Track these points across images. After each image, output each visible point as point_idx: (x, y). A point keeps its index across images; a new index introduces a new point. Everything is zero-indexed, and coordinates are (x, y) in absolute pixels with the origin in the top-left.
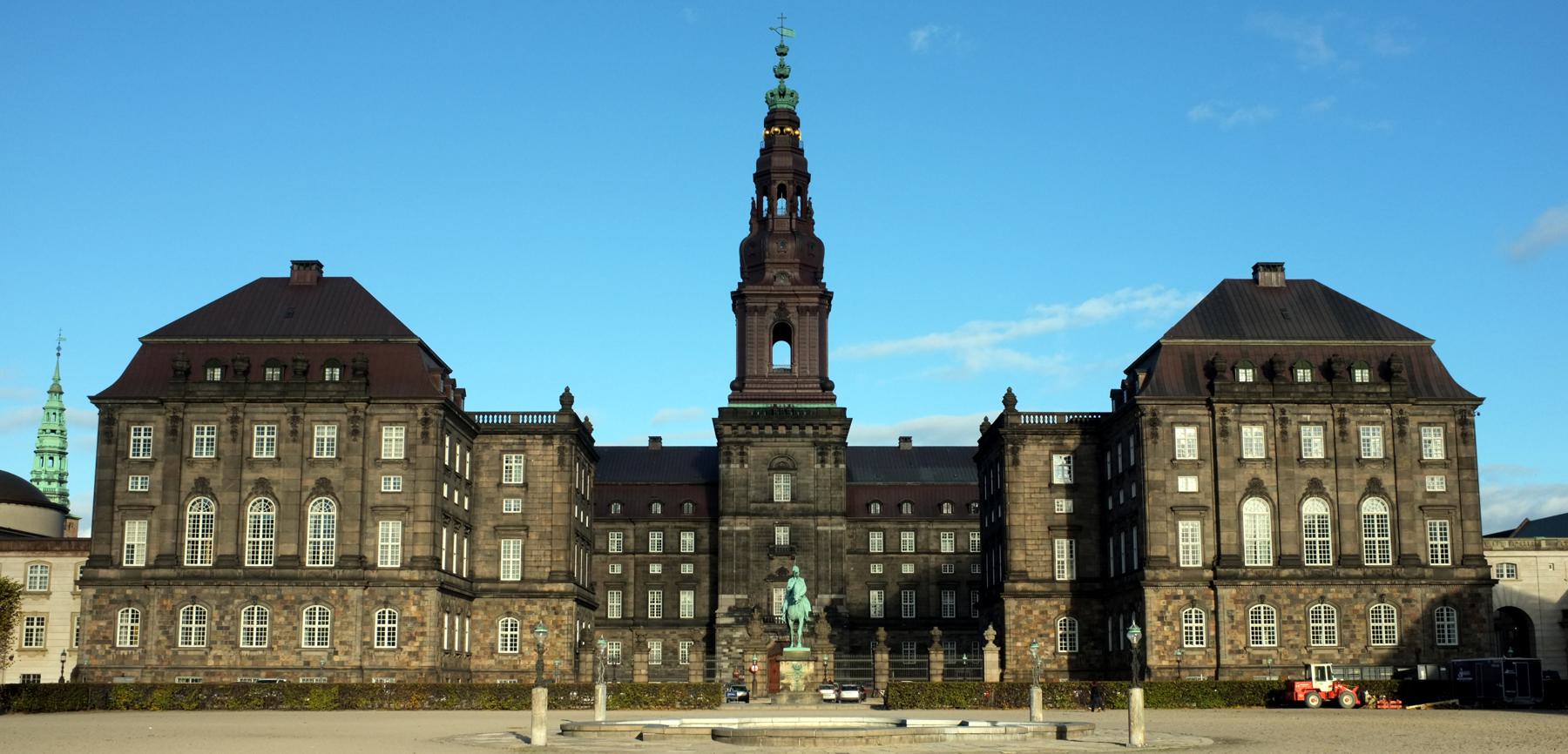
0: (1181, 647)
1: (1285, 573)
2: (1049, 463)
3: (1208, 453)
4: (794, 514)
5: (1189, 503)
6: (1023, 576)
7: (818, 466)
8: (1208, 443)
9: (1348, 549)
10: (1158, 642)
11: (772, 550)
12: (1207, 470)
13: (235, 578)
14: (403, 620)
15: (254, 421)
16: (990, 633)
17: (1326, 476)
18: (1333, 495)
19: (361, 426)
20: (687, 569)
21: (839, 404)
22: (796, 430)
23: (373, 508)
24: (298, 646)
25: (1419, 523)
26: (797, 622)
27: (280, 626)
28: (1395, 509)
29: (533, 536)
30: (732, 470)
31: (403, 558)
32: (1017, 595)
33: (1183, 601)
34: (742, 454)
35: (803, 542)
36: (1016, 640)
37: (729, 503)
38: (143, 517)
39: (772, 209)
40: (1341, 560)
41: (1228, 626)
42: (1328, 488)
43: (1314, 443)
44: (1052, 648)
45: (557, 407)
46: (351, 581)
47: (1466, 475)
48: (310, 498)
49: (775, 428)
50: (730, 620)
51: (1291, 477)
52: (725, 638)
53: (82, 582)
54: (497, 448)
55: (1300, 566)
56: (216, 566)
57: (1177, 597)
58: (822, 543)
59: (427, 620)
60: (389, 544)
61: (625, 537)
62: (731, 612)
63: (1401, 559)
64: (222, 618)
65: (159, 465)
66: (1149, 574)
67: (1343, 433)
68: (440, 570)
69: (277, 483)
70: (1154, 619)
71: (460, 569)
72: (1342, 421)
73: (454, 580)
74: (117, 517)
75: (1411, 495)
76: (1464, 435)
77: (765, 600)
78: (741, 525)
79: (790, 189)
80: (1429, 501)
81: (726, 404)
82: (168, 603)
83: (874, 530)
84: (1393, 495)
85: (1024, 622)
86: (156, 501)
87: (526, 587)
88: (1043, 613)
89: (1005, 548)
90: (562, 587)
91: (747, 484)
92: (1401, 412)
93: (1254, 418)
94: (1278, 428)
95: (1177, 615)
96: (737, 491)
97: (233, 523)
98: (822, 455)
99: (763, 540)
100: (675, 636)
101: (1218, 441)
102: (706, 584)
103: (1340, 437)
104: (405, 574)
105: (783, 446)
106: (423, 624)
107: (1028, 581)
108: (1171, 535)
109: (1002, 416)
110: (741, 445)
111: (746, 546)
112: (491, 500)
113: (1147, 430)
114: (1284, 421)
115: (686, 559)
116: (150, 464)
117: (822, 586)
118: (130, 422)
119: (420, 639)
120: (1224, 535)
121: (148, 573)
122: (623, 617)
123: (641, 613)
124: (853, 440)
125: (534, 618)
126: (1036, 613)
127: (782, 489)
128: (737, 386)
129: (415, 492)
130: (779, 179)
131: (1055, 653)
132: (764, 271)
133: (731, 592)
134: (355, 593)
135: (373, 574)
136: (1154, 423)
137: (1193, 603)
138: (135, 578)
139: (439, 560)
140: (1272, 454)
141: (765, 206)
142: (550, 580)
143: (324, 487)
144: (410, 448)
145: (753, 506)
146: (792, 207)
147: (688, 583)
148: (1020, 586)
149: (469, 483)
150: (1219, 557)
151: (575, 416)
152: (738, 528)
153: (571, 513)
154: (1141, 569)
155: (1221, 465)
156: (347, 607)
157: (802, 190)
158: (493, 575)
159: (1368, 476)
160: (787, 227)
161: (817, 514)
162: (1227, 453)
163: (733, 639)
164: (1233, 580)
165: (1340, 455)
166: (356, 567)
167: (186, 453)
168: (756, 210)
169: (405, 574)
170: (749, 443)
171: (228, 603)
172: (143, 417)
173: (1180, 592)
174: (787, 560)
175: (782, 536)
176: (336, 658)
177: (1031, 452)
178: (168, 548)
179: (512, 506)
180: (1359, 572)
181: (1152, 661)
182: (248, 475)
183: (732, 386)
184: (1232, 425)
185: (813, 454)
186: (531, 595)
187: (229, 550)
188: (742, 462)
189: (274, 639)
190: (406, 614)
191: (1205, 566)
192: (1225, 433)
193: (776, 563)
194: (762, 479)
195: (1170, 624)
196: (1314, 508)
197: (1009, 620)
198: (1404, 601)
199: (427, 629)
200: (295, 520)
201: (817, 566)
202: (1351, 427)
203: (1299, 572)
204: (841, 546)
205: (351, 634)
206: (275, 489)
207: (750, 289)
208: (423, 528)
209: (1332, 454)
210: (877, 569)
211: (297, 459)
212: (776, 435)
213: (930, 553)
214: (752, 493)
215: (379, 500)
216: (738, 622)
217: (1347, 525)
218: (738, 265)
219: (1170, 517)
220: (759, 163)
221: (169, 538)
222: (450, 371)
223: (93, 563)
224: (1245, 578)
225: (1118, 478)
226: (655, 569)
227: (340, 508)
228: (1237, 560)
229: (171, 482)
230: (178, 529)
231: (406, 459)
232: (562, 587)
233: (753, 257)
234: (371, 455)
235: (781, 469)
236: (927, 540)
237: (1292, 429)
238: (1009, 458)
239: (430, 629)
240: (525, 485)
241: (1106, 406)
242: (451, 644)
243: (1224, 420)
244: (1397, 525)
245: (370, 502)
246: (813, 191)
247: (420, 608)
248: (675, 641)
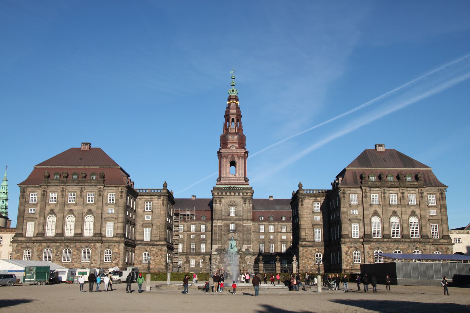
0: (353, 263)
1: (385, 240)
2: (312, 205)
3: (361, 203)
4: (236, 220)
5: (355, 218)
6: (305, 240)
7: (244, 205)
8: (361, 199)
9: (405, 233)
10: (346, 261)
11: (229, 231)
12: (361, 208)
13: (61, 240)
14: (113, 253)
15: (69, 192)
16: (295, 258)
17: (398, 210)
18: (400, 216)
19: (102, 193)
20: (203, 237)
22: (237, 194)
23: (105, 218)
24: (80, 261)
25: (428, 225)
26: (233, 254)
27: (75, 255)
28: (420, 220)
29: (154, 227)
30: (217, 206)
31: (114, 234)
32: (303, 246)
33: (353, 248)
34: (220, 201)
35: (239, 228)
36: (302, 260)
37: (216, 216)
38: (33, 221)
40: (403, 236)
41: (368, 257)
42: (399, 213)
43: (394, 199)
44: (314, 263)
45: (162, 187)
46: (97, 241)
47: (443, 210)
48: (85, 215)
49: (230, 193)
50: (216, 253)
51: (387, 210)
52: (214, 259)
53: (13, 242)
54: (144, 200)
55: (390, 238)
56: (56, 236)
57: (352, 247)
58: (245, 229)
59: (121, 253)
60: (110, 230)
61: (184, 227)
62: (217, 250)
63: (422, 236)
64: (57, 252)
65: (39, 205)
66: (343, 240)
67: (403, 197)
68: (125, 238)
69: (75, 211)
70: (344, 254)
71: (131, 237)
72: (403, 193)
73: (130, 241)
74: (24, 221)
75: (425, 217)
76: (442, 197)
77: (227, 247)
78: (220, 223)
79: (235, 120)
80: (431, 218)
82: (40, 248)
83: (261, 225)
84: (419, 216)
85: (305, 255)
86: (37, 216)
87: (152, 243)
88: (311, 251)
89: (299, 231)
90: (163, 243)
91: (221, 211)
92: (421, 190)
93: (375, 192)
94: (383, 195)
95: (351, 253)
96: (218, 212)
97: (62, 223)
98: (245, 201)
99: (227, 228)
100: (199, 258)
101: (364, 199)
102: (209, 241)
103: (402, 197)
104: (114, 239)
105: (233, 199)
106: (119, 254)
107: (306, 241)
108: (349, 228)
109: (298, 191)
110: (220, 198)
111: (221, 230)
112: (141, 216)
113: (341, 196)
114: (384, 193)
115: (203, 234)
116: (36, 205)
117: (245, 242)
118: (30, 192)
119: (118, 259)
120: (366, 228)
121: (34, 239)
122: (183, 252)
123: (188, 251)
124: (254, 197)
125: (154, 252)
126: (309, 251)
128: (219, 179)
129: (118, 213)
131: (315, 264)
133: (216, 244)
134: (98, 245)
135: (104, 239)
136: (344, 193)
137: (356, 249)
138: (30, 240)
139: (125, 235)
140: (381, 203)
141: (228, 125)
142: (159, 241)
143: (90, 212)
144: (117, 200)
145: (223, 217)
147: (204, 241)
148: (304, 243)
149: (135, 211)
150: (364, 235)
151: (168, 191)
152: (219, 224)
153: (166, 220)
154: (340, 239)
155: (365, 206)
156: (96, 249)
157: (238, 120)
158: (142, 239)
159: (411, 210)
160: (234, 131)
161: (243, 220)
162: (366, 203)
163: (217, 259)
164: (369, 242)
165: (402, 203)
166: (99, 236)
167: (47, 202)
169: (114, 239)
170: (222, 198)
171: (59, 248)
172: (34, 190)
173: (352, 246)
174: (234, 234)
175: (232, 227)
176: (92, 265)
177: (307, 202)
178: (41, 231)
179: (148, 218)
180: (409, 240)
181: (344, 267)
182: (67, 208)
183: (217, 181)
184: (368, 194)
185: (242, 201)
186: (153, 245)
187: (60, 231)
188: (220, 203)
189: (73, 259)
190: (114, 251)
191: (360, 238)
192: (366, 196)
193: (231, 235)
194: (226, 209)
195: (349, 255)
196: (394, 220)
197: (300, 254)
198: (424, 249)
199: (120, 256)
200: (80, 223)
201: (243, 236)
202: (405, 195)
203: (390, 240)
204: (251, 230)
205: (97, 258)
206: (75, 212)
207: (223, 150)
208: (121, 225)
209: (399, 203)
210: (262, 237)
211: (82, 203)
213: (278, 232)
214: (223, 213)
215: (107, 216)
216: (218, 254)
217: (405, 225)
218: (220, 143)
219: (349, 222)
220: (226, 112)
221: (41, 228)
222: (129, 176)
223: (17, 235)
224: (373, 241)
225: (334, 210)
226: (193, 237)
227: (95, 218)
228: (370, 236)
229: (43, 210)
230: (44, 224)
231: (116, 203)
232: (163, 243)
233: (224, 142)
234: (104, 202)
235: (232, 206)
236: (277, 228)
237: (387, 195)
238: (300, 204)
239: (122, 256)
240: (152, 211)
241: (330, 188)
242: (128, 260)
243: (366, 192)
244: (421, 225)
245: (104, 216)
246: (242, 120)
247: (119, 249)
248: (199, 259)
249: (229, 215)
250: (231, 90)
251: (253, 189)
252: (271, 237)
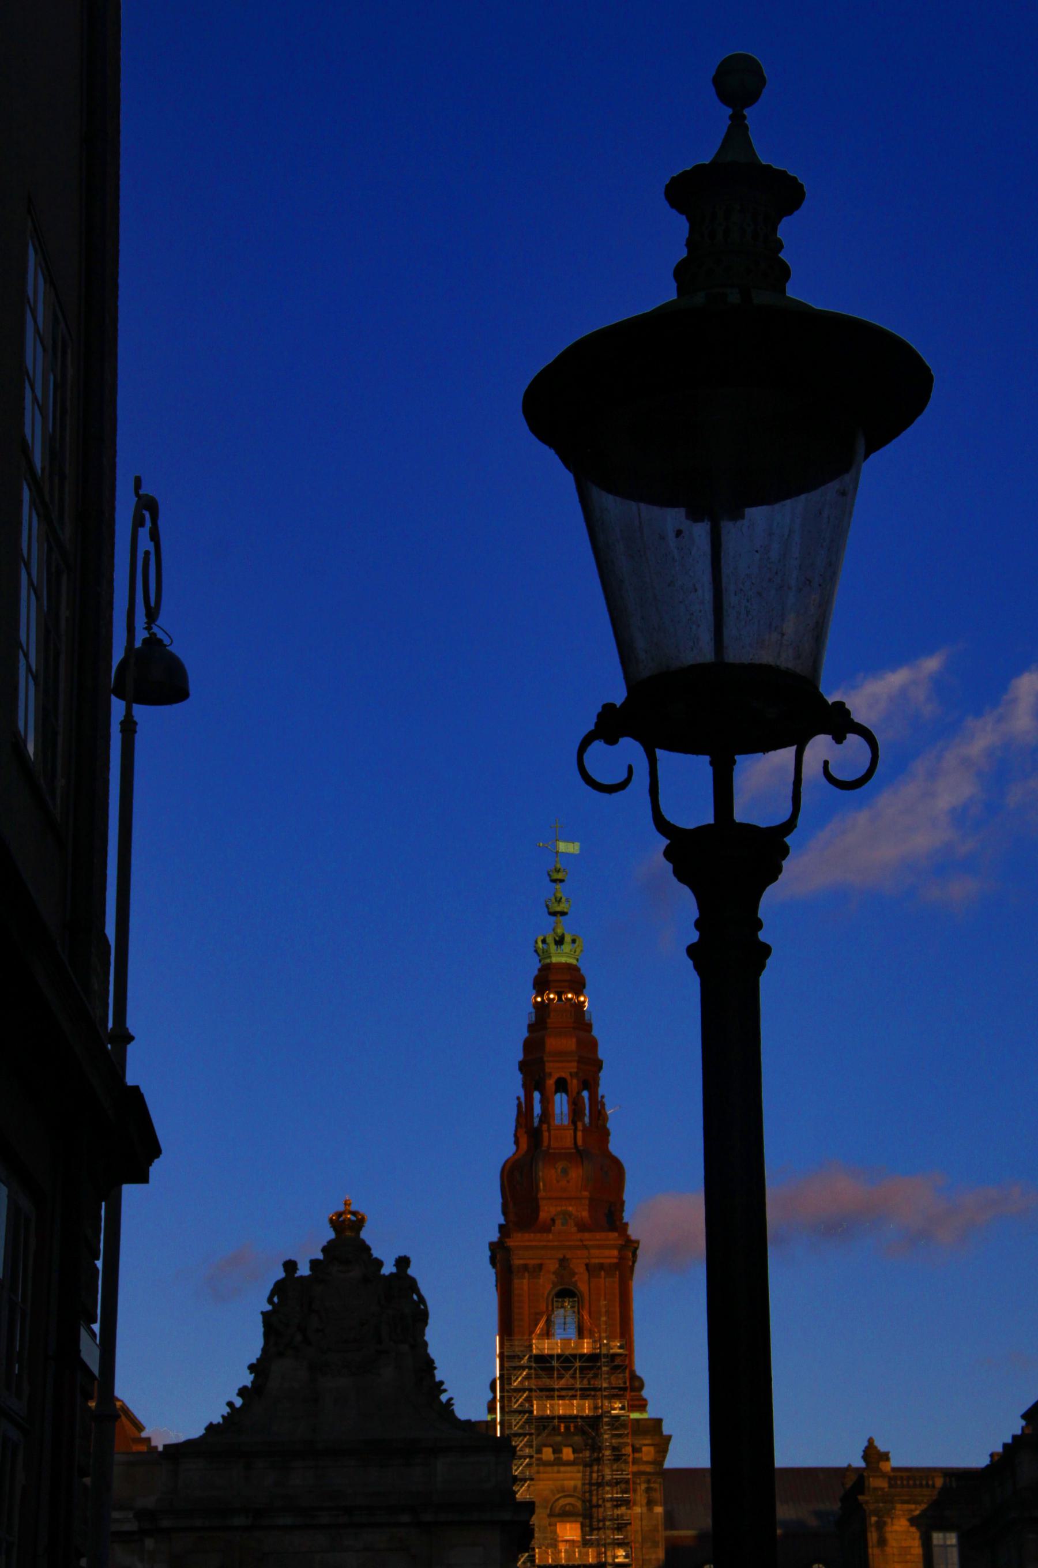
79: (574, 1084)
130: (555, 1070)
132: (536, 1210)
141: (537, 1110)
157: (590, 1083)
160: (569, 1142)
168: (524, 1113)
207: (516, 1240)
212: (559, 1462)
220: (529, 1046)
238: (873, 1536)
246: (607, 1085)
250: (550, 940)
251: (666, 1431)
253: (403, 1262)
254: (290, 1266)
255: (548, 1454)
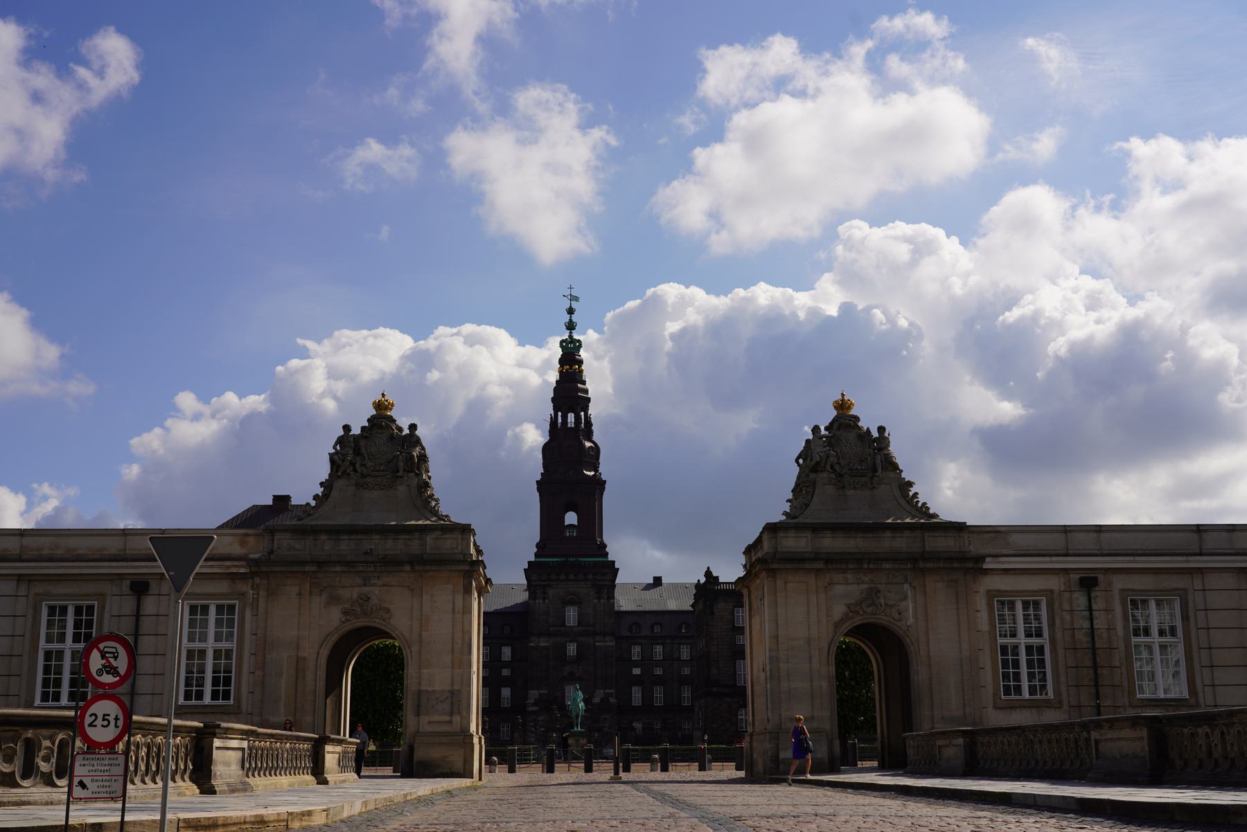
2: (732, 614)
20: (505, 672)
21: (610, 558)
26: (577, 716)
34: (544, 593)
39: (565, 418)
50: (535, 708)
62: (535, 704)
78: (544, 643)
81: (533, 559)
127: (571, 615)
141: (560, 420)
146: (578, 418)
147: (506, 682)
148: (714, 690)
157: (586, 409)
168: (553, 422)
175: (572, 649)
183: (537, 546)
188: (544, 599)
210: (636, 671)
235: (571, 603)
249: (563, 624)
252: (659, 671)
253: (413, 427)
254: (347, 428)
255: (563, 577)
